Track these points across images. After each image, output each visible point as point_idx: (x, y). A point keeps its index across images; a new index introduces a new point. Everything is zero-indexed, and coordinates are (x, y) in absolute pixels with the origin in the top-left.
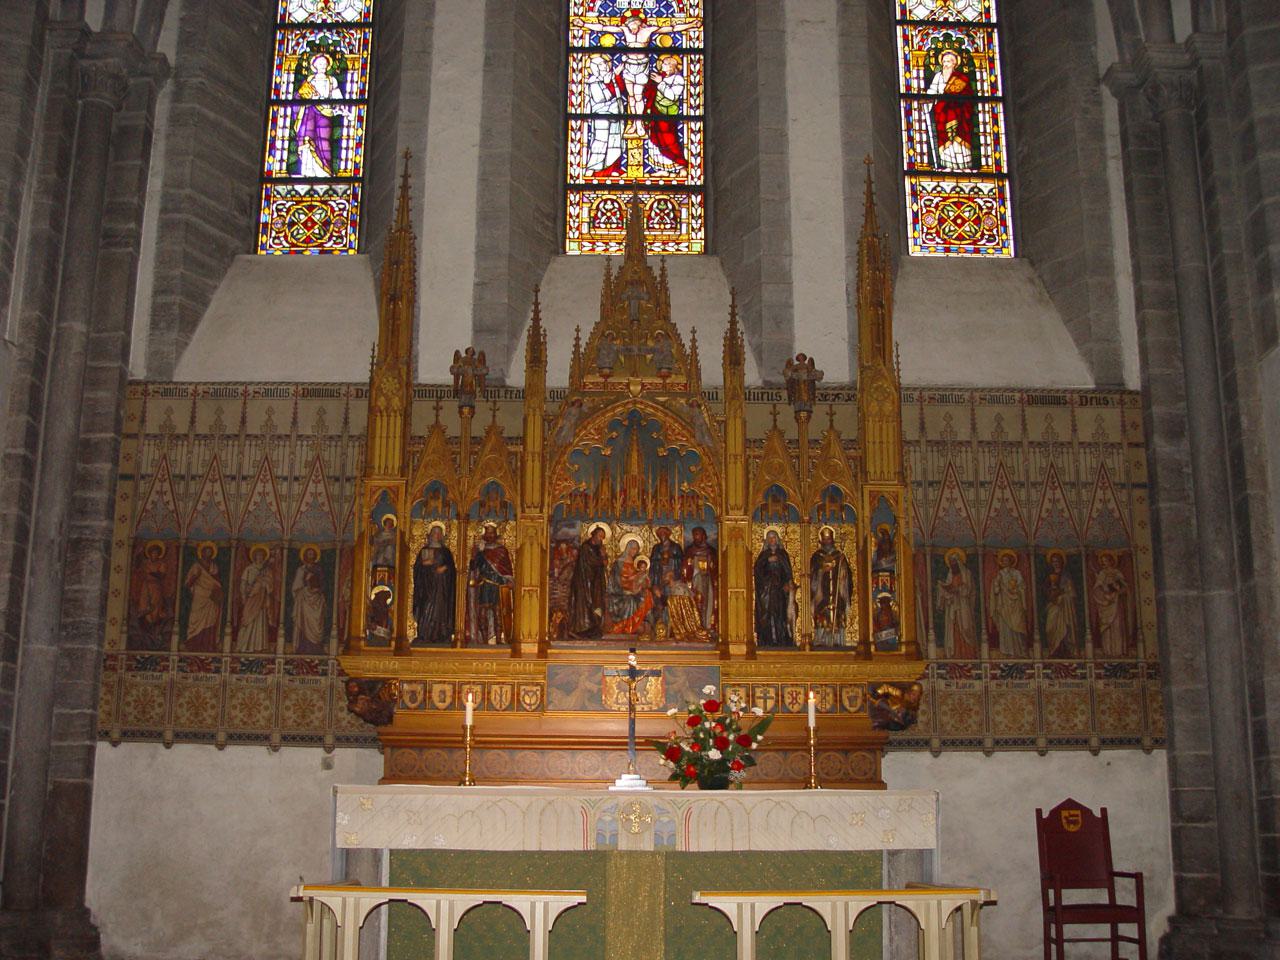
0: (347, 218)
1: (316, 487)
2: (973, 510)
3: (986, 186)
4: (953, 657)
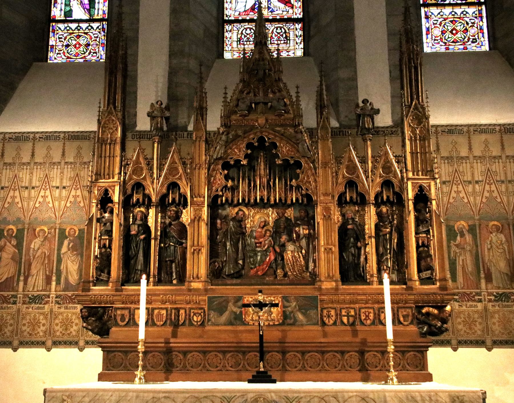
0: (99, 42)
1: (76, 192)
2: (472, 198)
3: (471, 10)
4: (462, 288)
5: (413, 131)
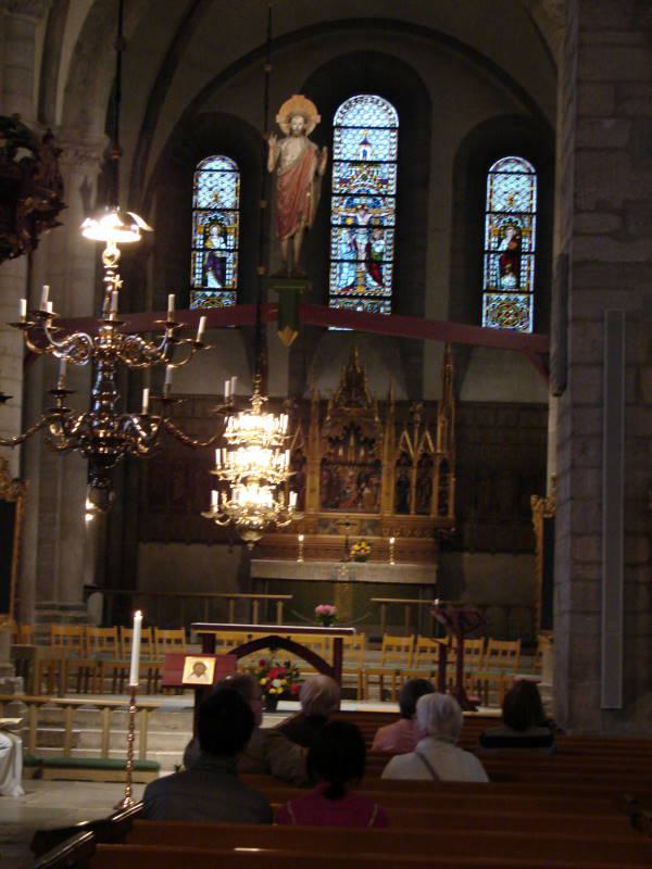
3: (522, 297)
5: (444, 422)
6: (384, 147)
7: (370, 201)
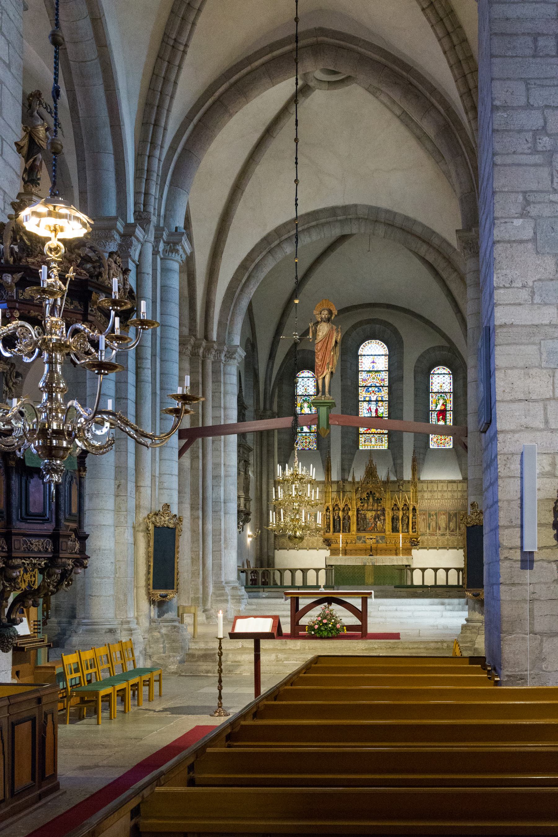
6: (382, 364)
7: (376, 389)
